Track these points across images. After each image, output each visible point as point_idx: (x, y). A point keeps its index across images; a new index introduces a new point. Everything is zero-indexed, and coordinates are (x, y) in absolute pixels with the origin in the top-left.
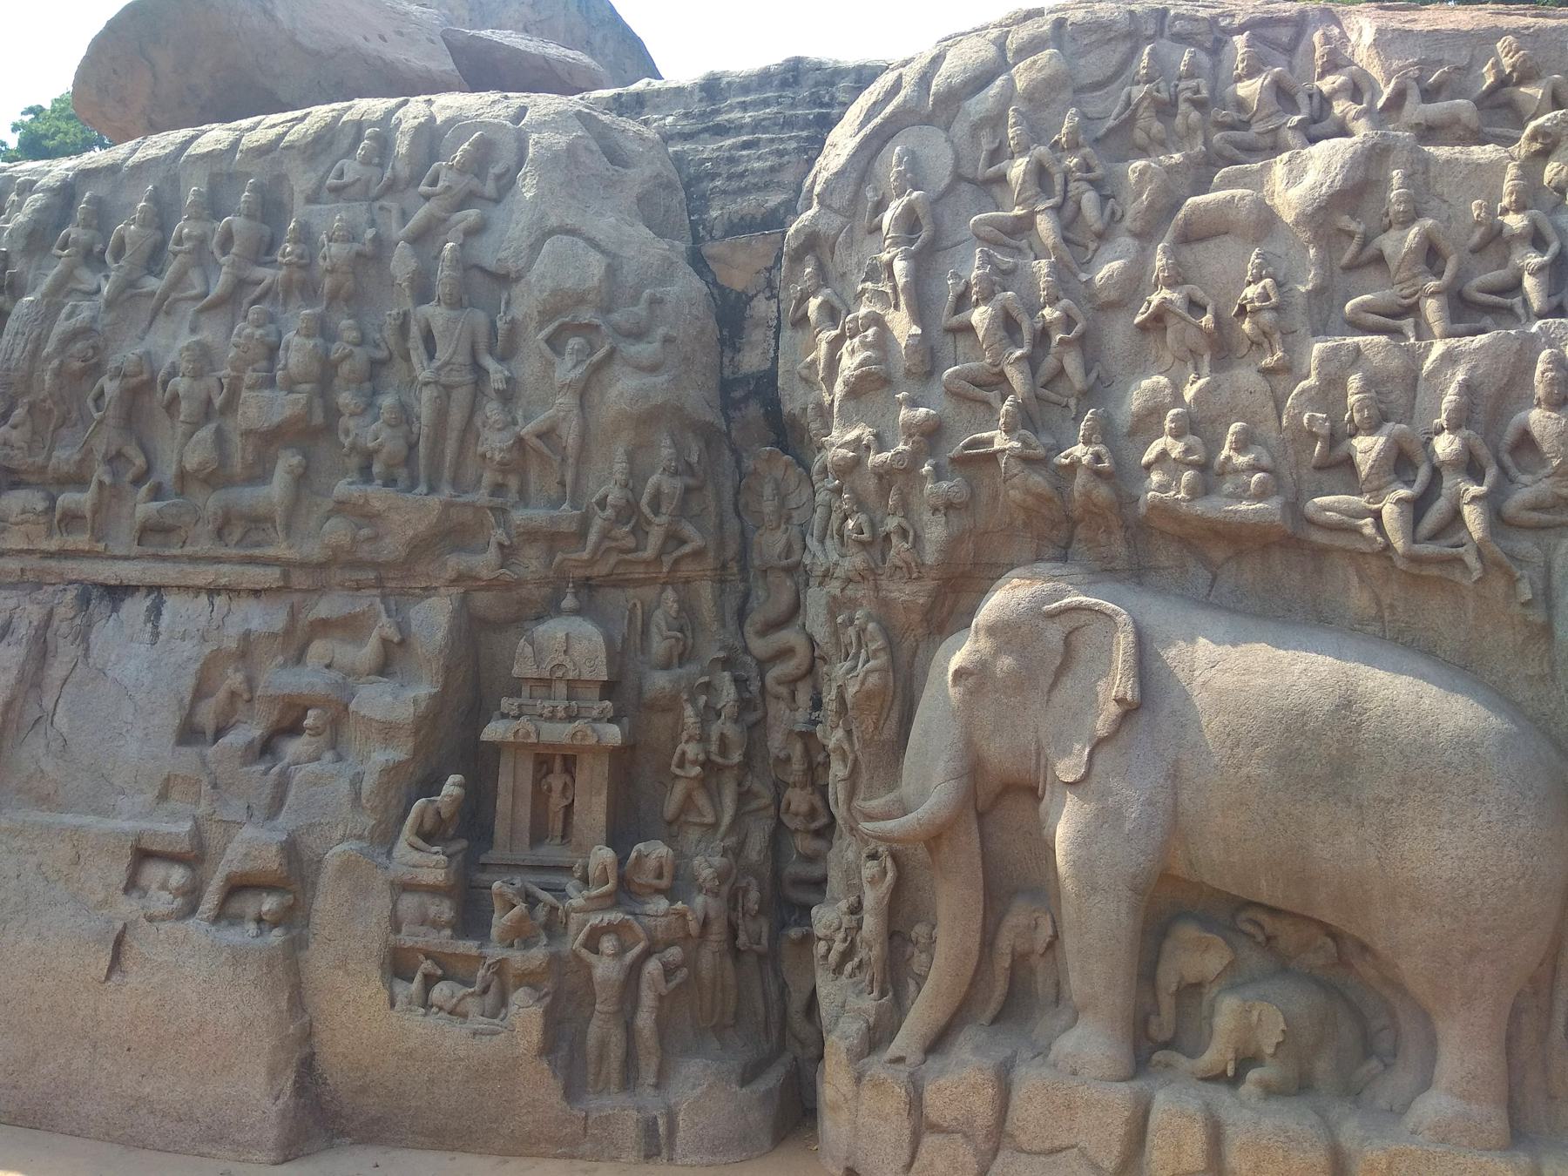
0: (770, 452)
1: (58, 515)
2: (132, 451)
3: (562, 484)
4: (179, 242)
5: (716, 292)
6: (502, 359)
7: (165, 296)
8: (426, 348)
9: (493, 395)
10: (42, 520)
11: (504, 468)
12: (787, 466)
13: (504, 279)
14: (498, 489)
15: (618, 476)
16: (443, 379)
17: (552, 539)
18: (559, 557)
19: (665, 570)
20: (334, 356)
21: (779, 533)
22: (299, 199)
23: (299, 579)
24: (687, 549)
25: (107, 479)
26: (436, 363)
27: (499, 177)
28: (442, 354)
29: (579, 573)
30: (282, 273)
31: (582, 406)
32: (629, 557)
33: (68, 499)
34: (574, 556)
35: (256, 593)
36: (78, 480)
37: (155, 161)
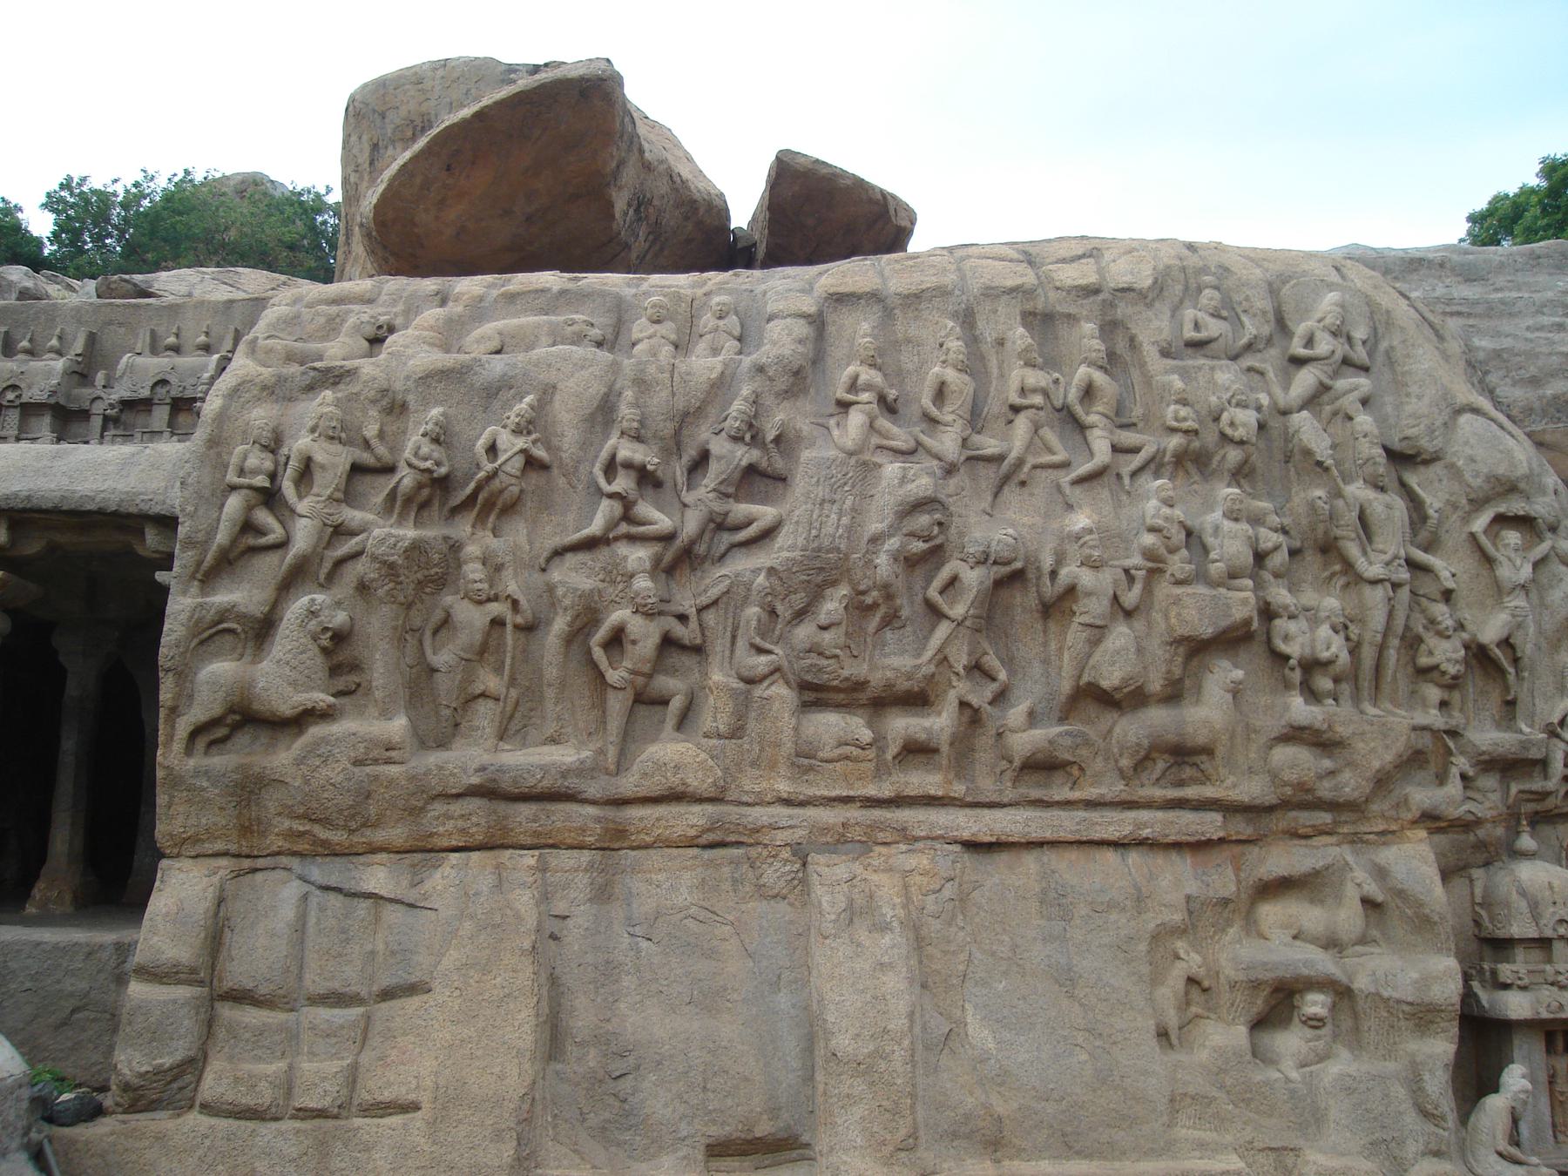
1: (893, 750)
2: (992, 661)
3: (1511, 704)
4: (1023, 391)
6: (1426, 550)
7: (1020, 463)
9: (1438, 597)
10: (871, 753)
11: (1454, 684)
13: (1402, 458)
14: (1443, 704)
16: (1394, 577)
17: (1507, 766)
18: (1514, 788)
20: (1265, 545)
22: (1150, 353)
23: (1241, 827)
25: (975, 701)
26: (1387, 557)
27: (1364, 343)
29: (1530, 807)
30: (1175, 442)
33: (902, 725)
34: (1537, 785)
35: (1177, 846)
36: (918, 700)
37: (942, 292)
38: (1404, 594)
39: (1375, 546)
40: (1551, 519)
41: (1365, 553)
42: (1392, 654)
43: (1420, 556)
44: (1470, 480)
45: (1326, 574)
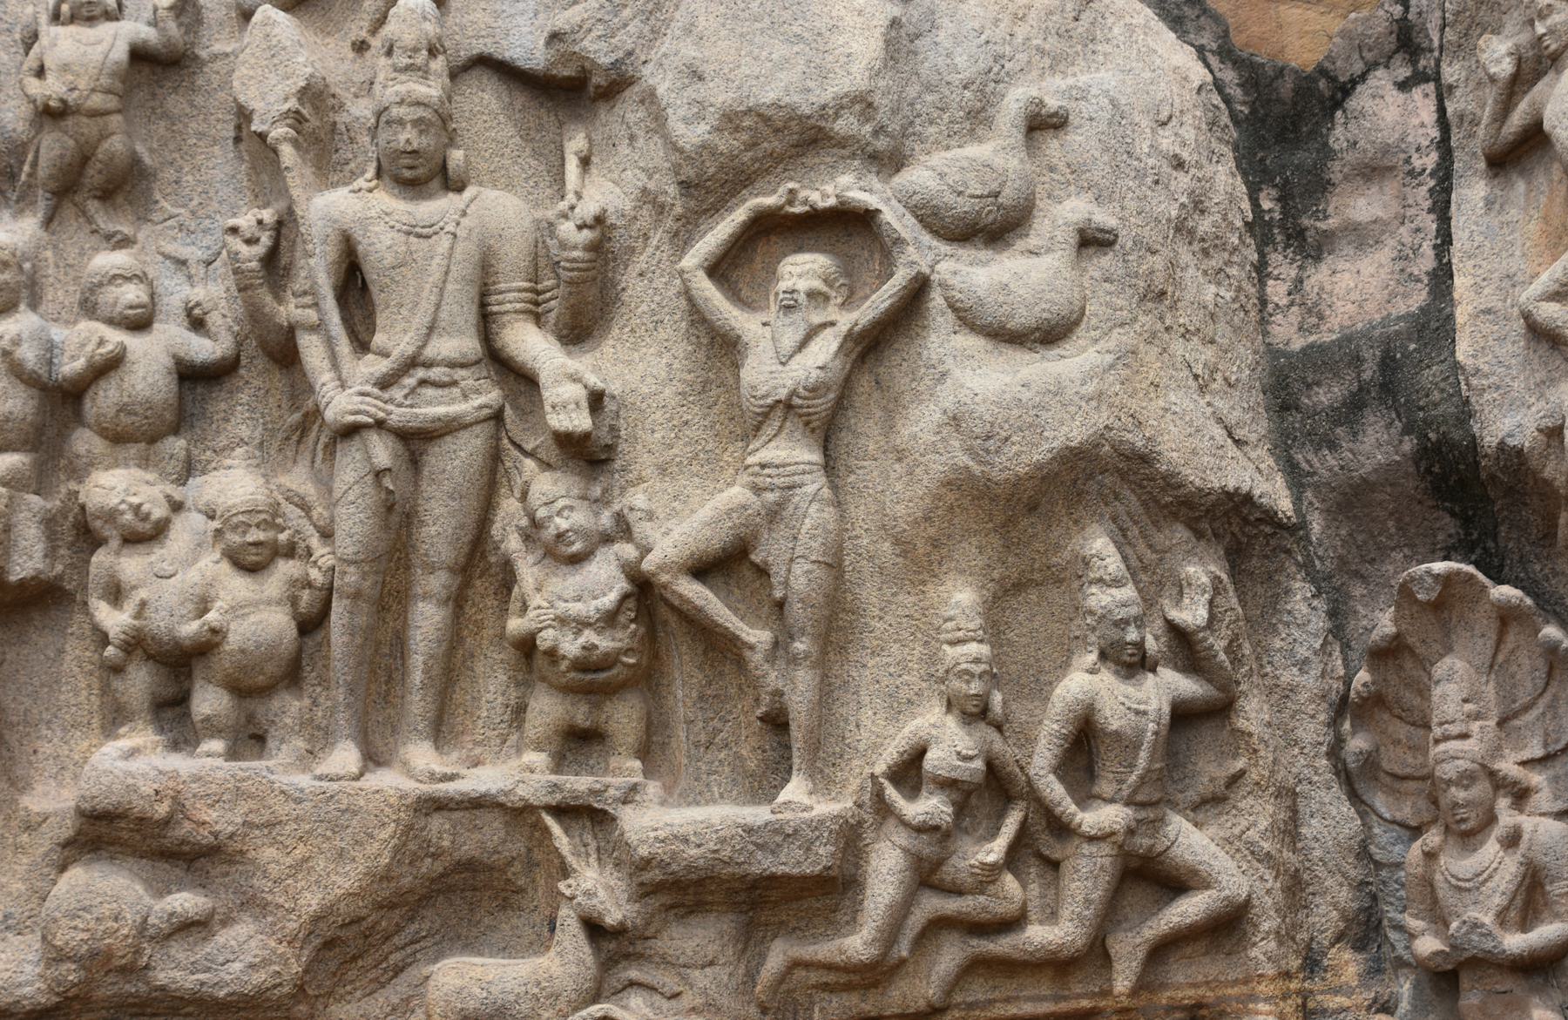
0: (1447, 580)
3: (777, 722)
5: (1229, 75)
8: (347, 321)
9: (552, 454)
11: (592, 679)
12: (1506, 617)
14: (579, 742)
15: (957, 684)
16: (398, 415)
18: (777, 956)
19: (1122, 983)
20: (71, 366)
21: (1491, 849)
24: (1189, 909)
26: (382, 366)
28: (396, 337)
31: (830, 467)
32: (1002, 945)
34: (823, 950)
38: (457, 460)
39: (379, 339)
40: (964, 205)
41: (335, 365)
42: (427, 620)
43: (531, 343)
44: (677, 127)
45: (297, 416)
